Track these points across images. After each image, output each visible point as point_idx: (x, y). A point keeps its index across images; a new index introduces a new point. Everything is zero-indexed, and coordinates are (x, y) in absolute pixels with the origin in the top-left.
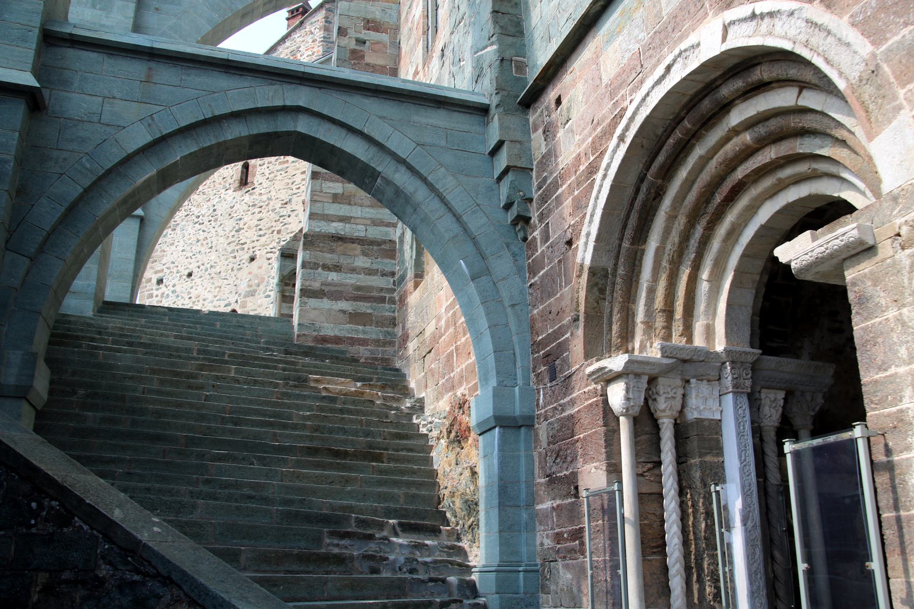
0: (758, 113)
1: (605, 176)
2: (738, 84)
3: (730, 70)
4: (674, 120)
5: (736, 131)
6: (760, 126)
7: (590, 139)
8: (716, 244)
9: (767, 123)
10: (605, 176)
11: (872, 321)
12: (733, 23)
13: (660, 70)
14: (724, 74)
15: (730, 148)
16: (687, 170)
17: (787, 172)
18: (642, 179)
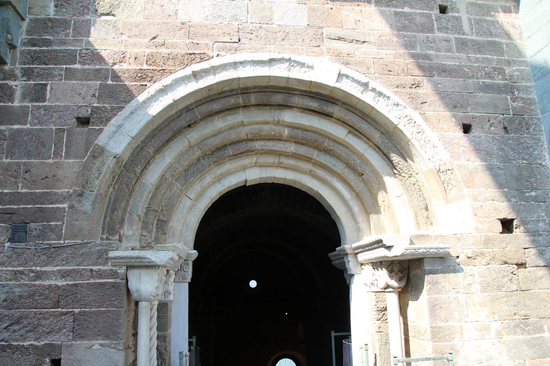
0: (310, 127)
1: (163, 91)
2: (314, 105)
3: (310, 92)
4: (242, 89)
5: (278, 123)
6: (300, 131)
7: (148, 51)
8: (208, 179)
9: (306, 133)
10: (163, 91)
11: (440, 296)
12: (347, 77)
13: (265, 57)
14: (305, 91)
15: (266, 128)
16: (225, 124)
17: (291, 162)
18: (188, 109)
